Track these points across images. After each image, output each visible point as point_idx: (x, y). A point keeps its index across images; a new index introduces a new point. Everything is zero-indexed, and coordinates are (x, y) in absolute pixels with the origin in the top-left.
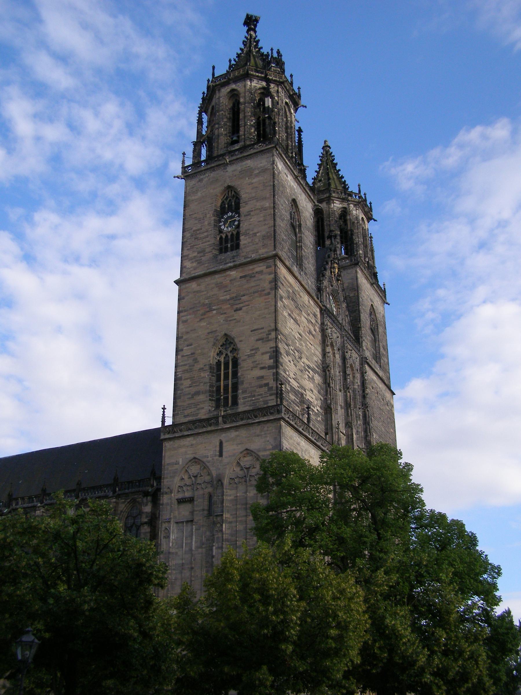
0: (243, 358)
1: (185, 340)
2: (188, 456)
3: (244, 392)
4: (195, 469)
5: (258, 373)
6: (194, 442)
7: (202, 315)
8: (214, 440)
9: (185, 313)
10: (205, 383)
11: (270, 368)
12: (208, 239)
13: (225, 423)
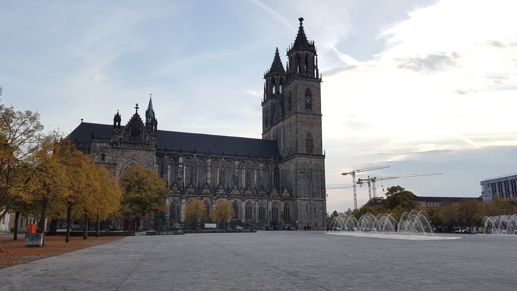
1: (299, 130)
4: (304, 165)
5: (318, 145)
7: (303, 125)
8: (309, 159)
11: (320, 145)
12: (303, 102)
13: (312, 156)
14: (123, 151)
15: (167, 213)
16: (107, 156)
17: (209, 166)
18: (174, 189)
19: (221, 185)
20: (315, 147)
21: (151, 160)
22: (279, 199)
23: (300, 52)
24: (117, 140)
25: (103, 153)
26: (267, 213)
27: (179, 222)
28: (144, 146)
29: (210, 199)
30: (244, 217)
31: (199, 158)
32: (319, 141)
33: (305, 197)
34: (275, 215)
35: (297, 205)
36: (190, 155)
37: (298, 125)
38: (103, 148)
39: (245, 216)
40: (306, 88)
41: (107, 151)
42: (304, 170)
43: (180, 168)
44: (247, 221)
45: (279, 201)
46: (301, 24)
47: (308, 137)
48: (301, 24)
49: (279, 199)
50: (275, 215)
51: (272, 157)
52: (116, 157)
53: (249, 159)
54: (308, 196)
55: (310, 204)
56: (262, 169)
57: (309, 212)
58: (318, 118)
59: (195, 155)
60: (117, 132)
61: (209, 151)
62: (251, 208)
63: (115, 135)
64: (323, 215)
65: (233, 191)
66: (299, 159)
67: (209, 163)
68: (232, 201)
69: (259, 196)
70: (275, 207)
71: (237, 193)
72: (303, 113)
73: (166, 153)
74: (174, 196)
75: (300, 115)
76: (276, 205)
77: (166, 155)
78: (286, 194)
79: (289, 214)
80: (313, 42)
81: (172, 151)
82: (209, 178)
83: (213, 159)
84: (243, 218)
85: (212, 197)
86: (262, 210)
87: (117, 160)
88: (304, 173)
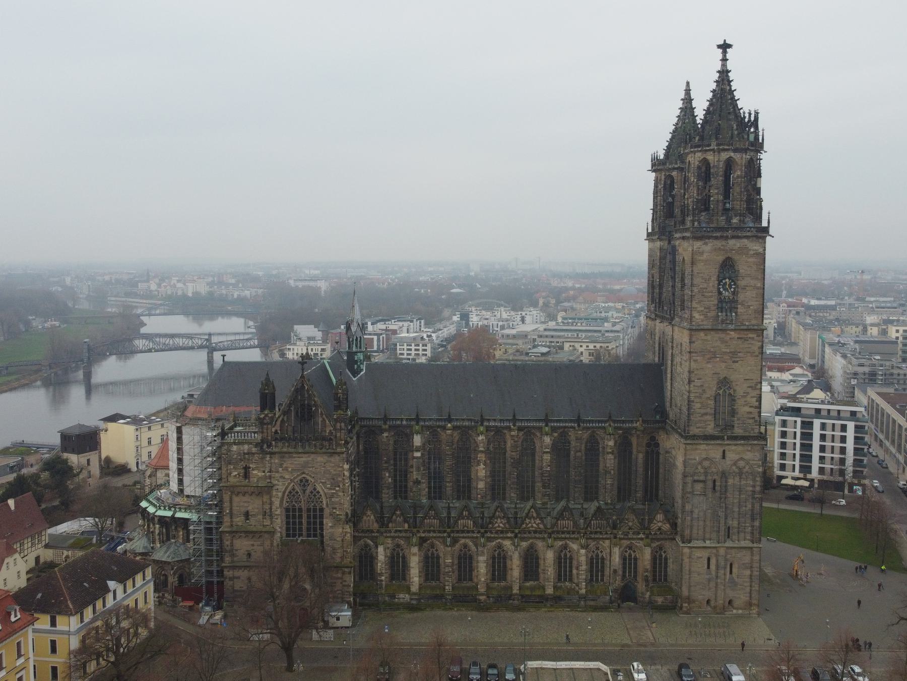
0: (738, 397)
1: (696, 374)
2: (702, 456)
3: (738, 419)
5: (747, 409)
6: (707, 448)
7: (708, 359)
10: (711, 408)
11: (756, 407)
13: (728, 439)
14: (283, 457)
15: (381, 574)
16: (253, 470)
17: (482, 452)
18: (395, 520)
19: (499, 509)
20: (739, 416)
21: (338, 472)
22: (642, 539)
23: (710, 157)
24: (270, 435)
25: (246, 465)
26: (608, 569)
27: (408, 590)
28: (322, 445)
29: (473, 542)
30: (551, 582)
31: (459, 431)
32: (752, 397)
33: (704, 541)
34: (630, 572)
35: (682, 560)
36: (439, 427)
37: (694, 361)
38: (244, 454)
39: (552, 580)
40: (721, 258)
41: (252, 460)
42: (706, 476)
43: (417, 458)
45: (640, 544)
46: (724, 60)
47: (722, 391)
48: (724, 60)
49: (642, 539)
50: (630, 572)
51: (640, 419)
52: (270, 472)
53: (579, 426)
54: (714, 535)
55: (717, 556)
57: (714, 573)
58: (753, 338)
59: (449, 425)
60: (267, 418)
61: (482, 416)
62: (571, 558)
63: (265, 426)
64: (751, 582)
65: (528, 521)
67: (482, 445)
68: (524, 544)
69: (591, 533)
70: (630, 555)
71: (538, 525)
72: (710, 327)
73: (387, 427)
74: (396, 537)
75: (702, 334)
76: (634, 552)
77: (385, 431)
78: (660, 524)
79: (666, 571)
80: (758, 113)
81: (398, 419)
82: (481, 477)
83: (491, 431)
85: (477, 537)
86: (597, 563)
87: (274, 477)
88: (704, 482)
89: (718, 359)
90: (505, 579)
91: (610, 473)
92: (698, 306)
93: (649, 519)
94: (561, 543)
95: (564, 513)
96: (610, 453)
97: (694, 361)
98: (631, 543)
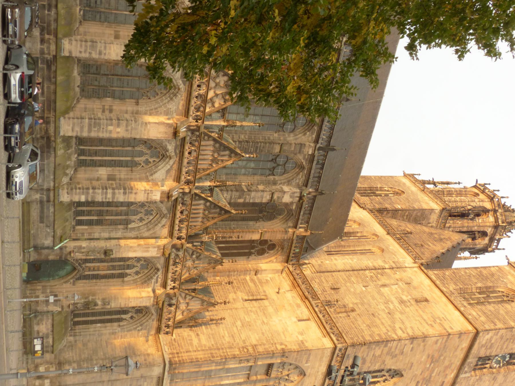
7: (433, 356)
9: (444, 341)
10: (369, 367)
26: (106, 235)
30: (90, 131)
37: (438, 340)
44: (68, 146)
51: (308, 233)
53: (320, 149)
56: (275, 197)
62: (132, 165)
66: (322, 358)
76: (137, 273)
78: (183, 306)
84: (86, 129)
89: (428, 366)
90: (85, 18)
91: (240, 198)
92: (498, 337)
93: (194, 290)
94: (171, 148)
95: (227, 152)
96: (272, 197)
97: (438, 340)
98: (158, 270)
